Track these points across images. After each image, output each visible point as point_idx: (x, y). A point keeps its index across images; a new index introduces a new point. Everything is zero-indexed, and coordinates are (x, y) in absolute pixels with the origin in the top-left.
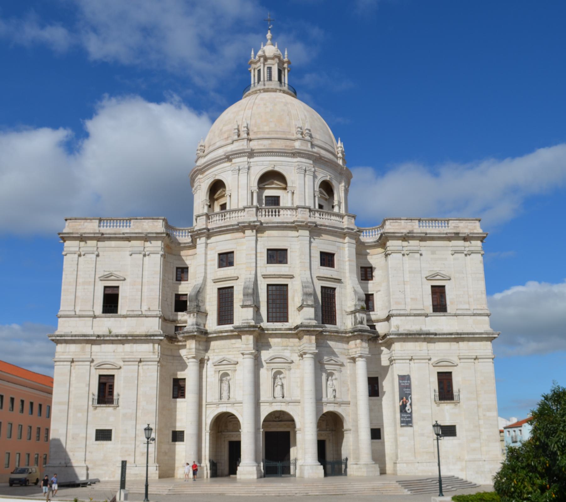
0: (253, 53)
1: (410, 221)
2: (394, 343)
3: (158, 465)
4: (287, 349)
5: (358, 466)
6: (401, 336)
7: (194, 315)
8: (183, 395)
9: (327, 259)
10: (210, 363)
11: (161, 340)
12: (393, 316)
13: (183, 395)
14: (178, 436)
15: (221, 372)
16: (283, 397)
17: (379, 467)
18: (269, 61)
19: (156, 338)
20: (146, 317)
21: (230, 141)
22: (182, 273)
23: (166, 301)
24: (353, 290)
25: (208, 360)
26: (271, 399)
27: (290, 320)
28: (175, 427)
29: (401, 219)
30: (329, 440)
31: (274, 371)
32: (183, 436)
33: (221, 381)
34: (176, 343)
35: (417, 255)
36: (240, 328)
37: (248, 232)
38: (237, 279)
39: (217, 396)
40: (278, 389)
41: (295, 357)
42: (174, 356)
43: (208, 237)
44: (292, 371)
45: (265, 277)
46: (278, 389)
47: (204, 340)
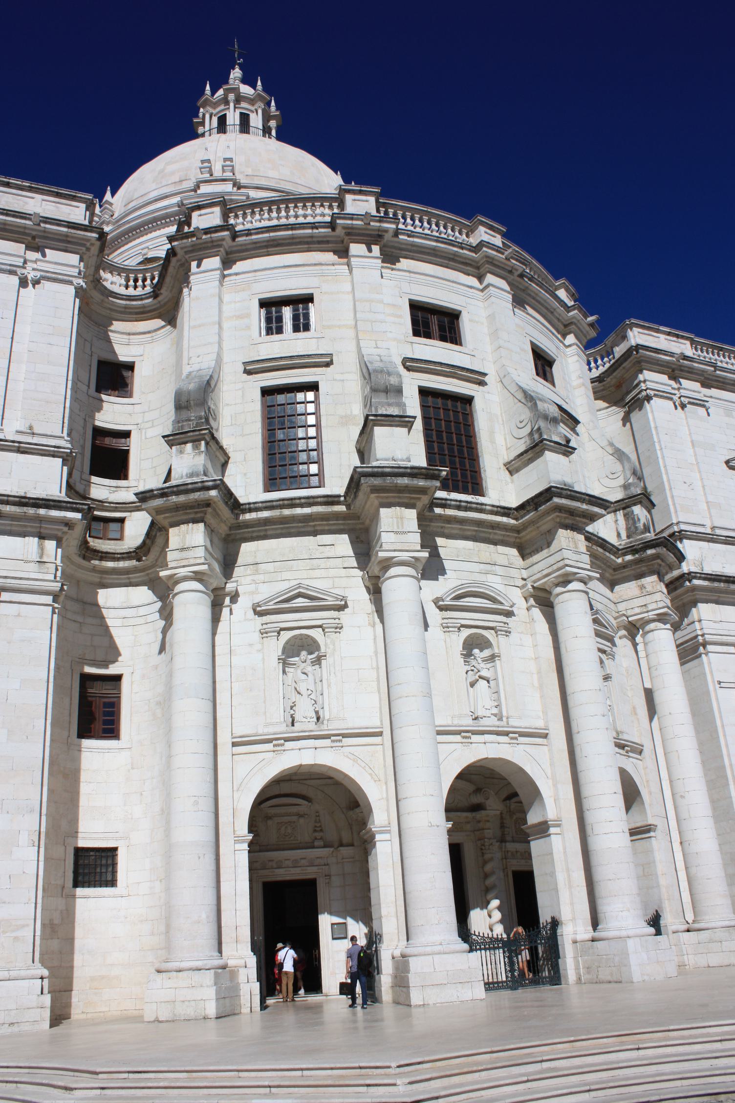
0: (208, 87)
1: (675, 339)
2: (694, 604)
3: (45, 972)
5: (703, 935)
6: (716, 584)
7: (196, 448)
8: (111, 731)
11: (69, 524)
12: (681, 535)
13: (111, 731)
14: (94, 867)
15: (286, 636)
18: (243, 105)
19: (55, 513)
20: (21, 449)
21: (190, 184)
22: (114, 377)
25: (235, 597)
26: (471, 722)
28: (75, 834)
29: (658, 331)
31: (466, 632)
32: (114, 865)
34: (96, 562)
35: (701, 411)
36: (384, 475)
37: (357, 249)
38: (328, 365)
41: (516, 598)
42: (85, 603)
43: (227, 263)
45: (411, 364)
47: (223, 529)
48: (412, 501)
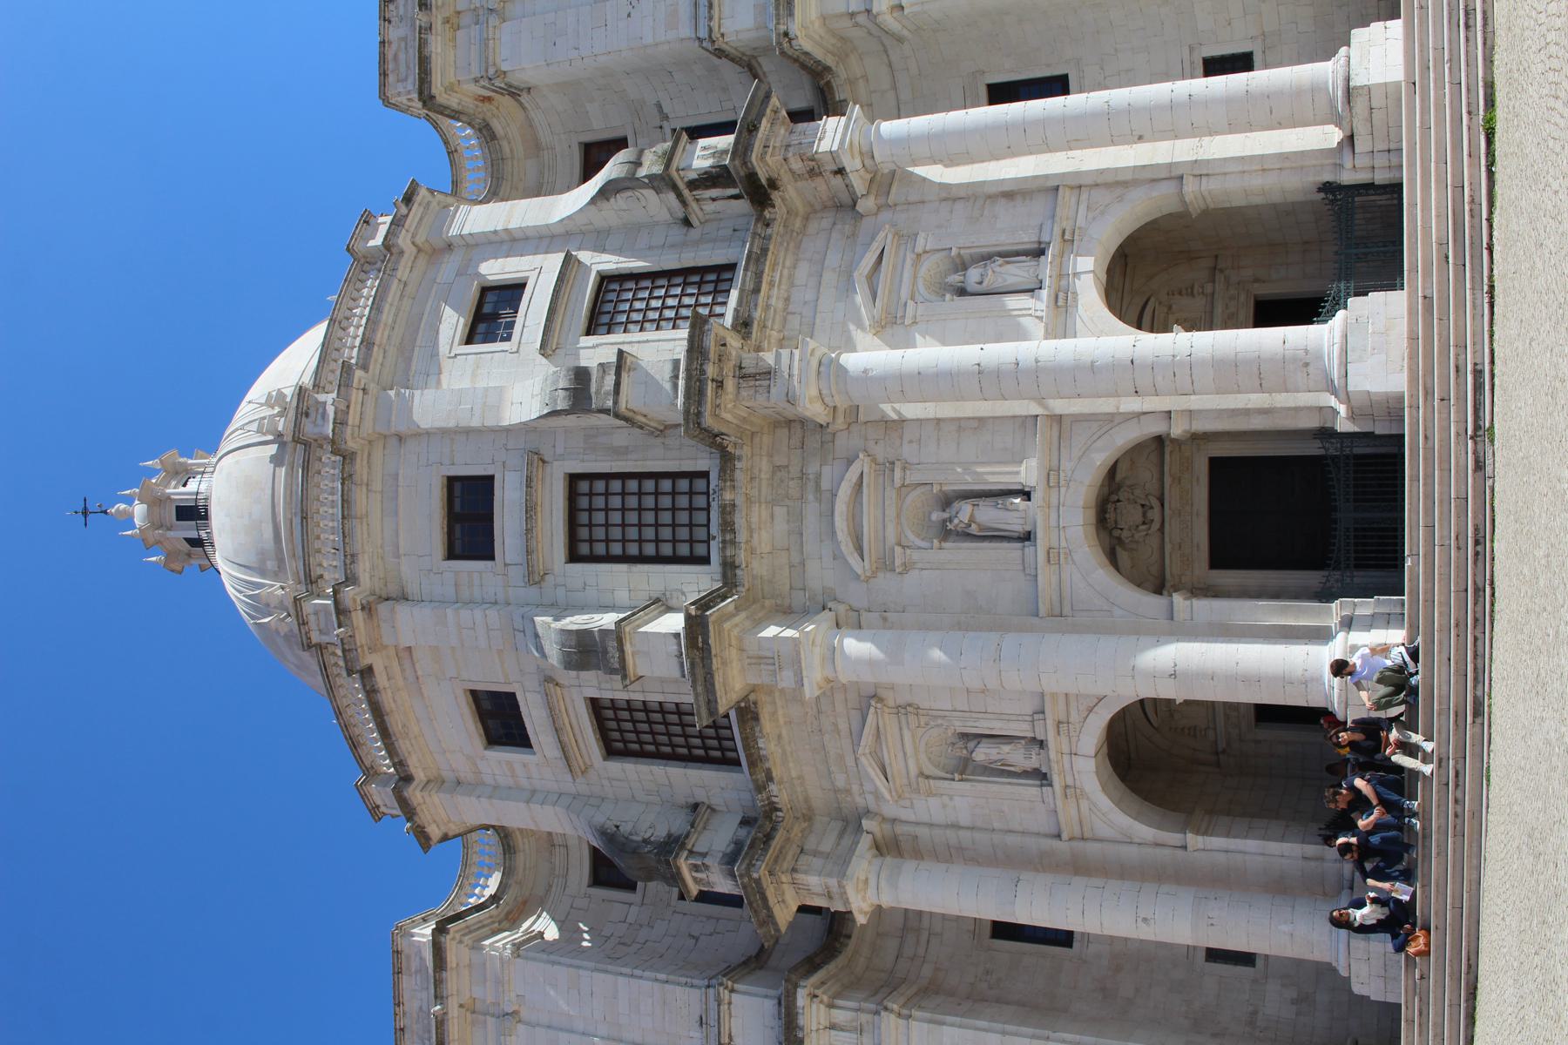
4: (819, 476)
7: (696, 868)
9: (492, 313)
10: (890, 810)
16: (1026, 495)
17: (1365, 23)
23: (697, 939)
24: (604, 205)
27: (701, 465)
30: (1257, 280)
33: (964, 768)
39: (1029, 791)
40: (988, 515)
42: (905, 928)
44: (908, 452)
46: (988, 515)
48: (734, 642)
